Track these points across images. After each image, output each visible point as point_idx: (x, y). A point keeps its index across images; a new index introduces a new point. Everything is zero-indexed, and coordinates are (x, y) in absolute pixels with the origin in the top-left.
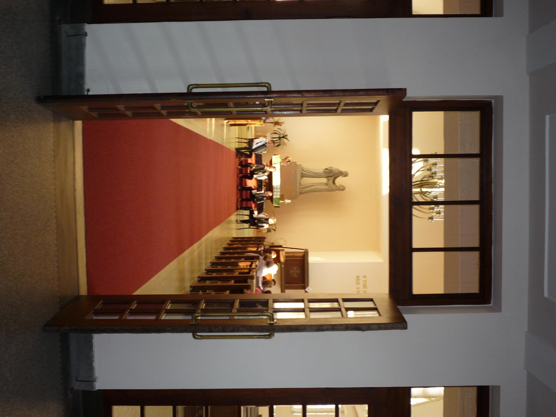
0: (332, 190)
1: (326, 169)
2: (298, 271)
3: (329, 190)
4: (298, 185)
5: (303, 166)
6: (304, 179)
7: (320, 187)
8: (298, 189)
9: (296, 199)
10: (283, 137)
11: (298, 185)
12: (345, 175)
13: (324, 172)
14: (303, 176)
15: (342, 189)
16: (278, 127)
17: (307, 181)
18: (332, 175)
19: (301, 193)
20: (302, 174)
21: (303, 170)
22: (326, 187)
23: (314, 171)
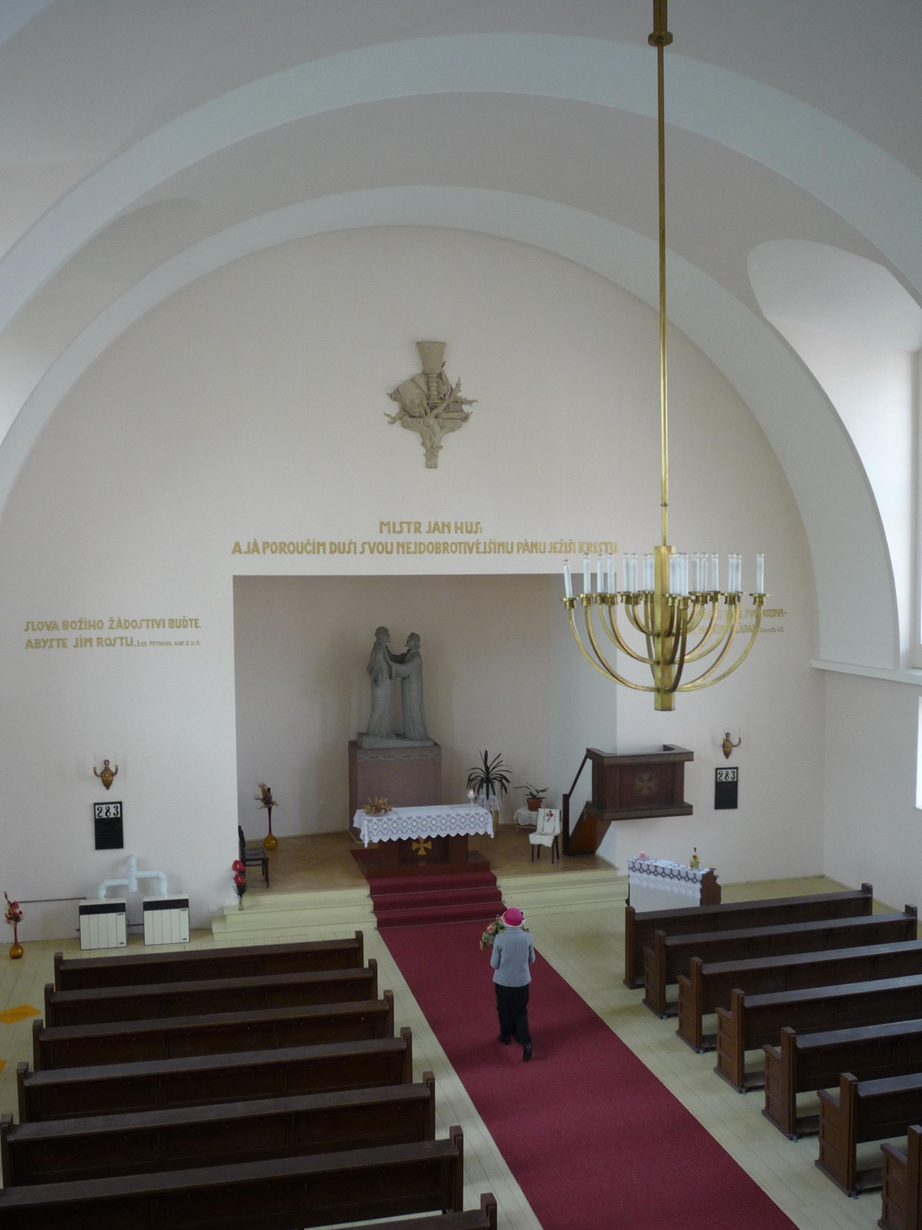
2: (646, 776)
3: (420, 673)
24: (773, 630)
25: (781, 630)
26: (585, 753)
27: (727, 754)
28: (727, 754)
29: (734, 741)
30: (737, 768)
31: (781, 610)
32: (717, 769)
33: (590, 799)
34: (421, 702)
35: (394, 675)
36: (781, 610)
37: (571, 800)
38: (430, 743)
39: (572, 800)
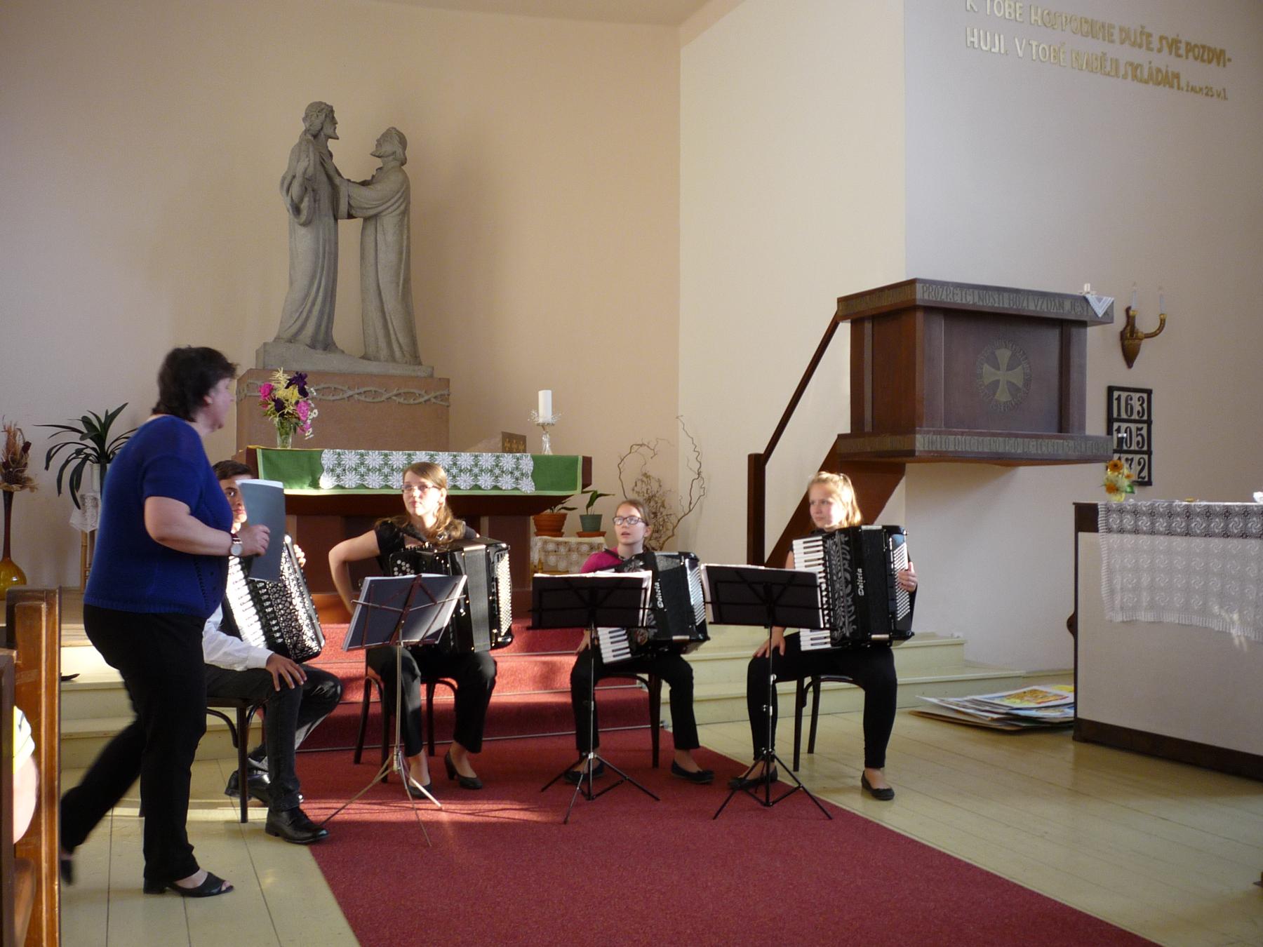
0: (404, 193)
1: (297, 210)
3: (405, 212)
4: (372, 367)
5: (270, 339)
6: (345, 329)
7: (387, 256)
8: (393, 369)
9: (446, 382)
10: (100, 438)
11: (372, 367)
12: (321, 124)
13: (304, 225)
14: (324, 342)
15: (393, 148)
16: (34, 466)
17: (347, 325)
18: (320, 192)
19: (416, 359)
20: (313, 346)
21: (292, 339)
22: (389, 222)
23: (302, 282)
24: (1208, 92)
25: (1222, 95)
26: (832, 309)
27: (1130, 356)
28: (1130, 356)
29: (1145, 324)
30: (1149, 392)
31: (1222, 52)
32: (1111, 390)
33: (846, 429)
34: (407, 280)
35: (343, 208)
36: (1222, 52)
37: (770, 468)
38: (421, 372)
39: (772, 469)
